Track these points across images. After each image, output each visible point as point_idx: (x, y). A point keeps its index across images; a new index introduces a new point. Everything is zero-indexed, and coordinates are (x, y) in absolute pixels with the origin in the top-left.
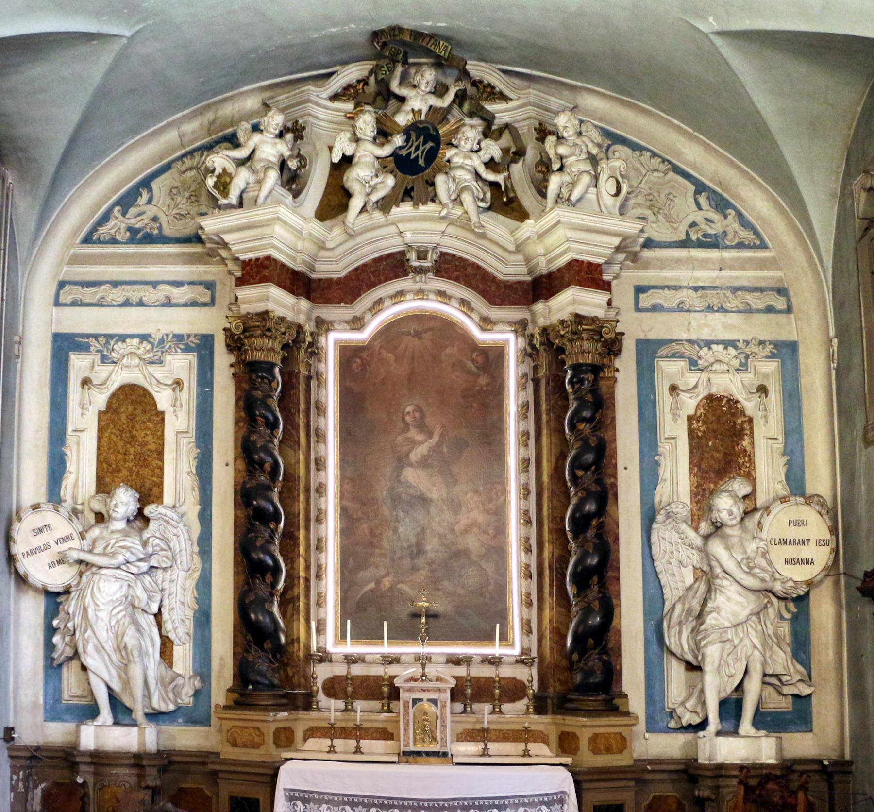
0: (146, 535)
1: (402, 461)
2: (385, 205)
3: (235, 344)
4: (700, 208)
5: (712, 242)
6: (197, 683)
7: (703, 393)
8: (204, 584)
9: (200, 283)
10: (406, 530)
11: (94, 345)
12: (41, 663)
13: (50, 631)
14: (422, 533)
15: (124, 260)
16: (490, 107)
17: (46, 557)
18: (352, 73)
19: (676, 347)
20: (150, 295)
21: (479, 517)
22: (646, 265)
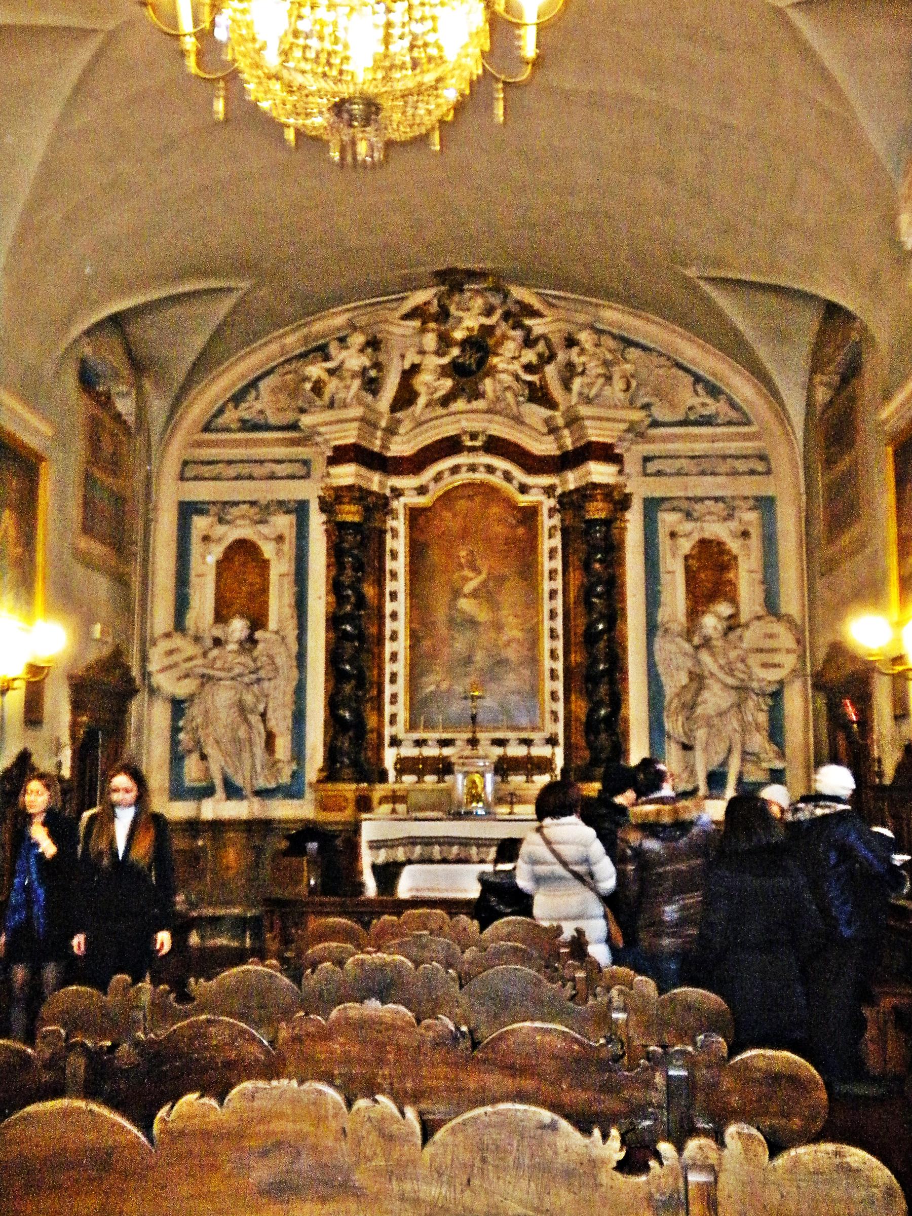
0: (256, 653)
1: (457, 593)
2: (445, 401)
3: (326, 507)
4: (697, 394)
5: (706, 421)
6: (294, 767)
7: (696, 537)
8: (300, 691)
9: (297, 461)
10: (460, 645)
11: (214, 509)
12: (167, 756)
13: (175, 730)
14: (472, 648)
15: (237, 444)
16: (528, 322)
17: (175, 673)
18: (419, 297)
19: (676, 503)
20: (257, 470)
21: (517, 634)
22: (652, 440)
